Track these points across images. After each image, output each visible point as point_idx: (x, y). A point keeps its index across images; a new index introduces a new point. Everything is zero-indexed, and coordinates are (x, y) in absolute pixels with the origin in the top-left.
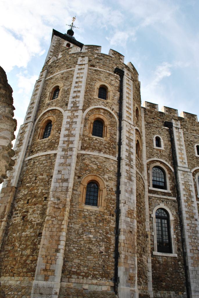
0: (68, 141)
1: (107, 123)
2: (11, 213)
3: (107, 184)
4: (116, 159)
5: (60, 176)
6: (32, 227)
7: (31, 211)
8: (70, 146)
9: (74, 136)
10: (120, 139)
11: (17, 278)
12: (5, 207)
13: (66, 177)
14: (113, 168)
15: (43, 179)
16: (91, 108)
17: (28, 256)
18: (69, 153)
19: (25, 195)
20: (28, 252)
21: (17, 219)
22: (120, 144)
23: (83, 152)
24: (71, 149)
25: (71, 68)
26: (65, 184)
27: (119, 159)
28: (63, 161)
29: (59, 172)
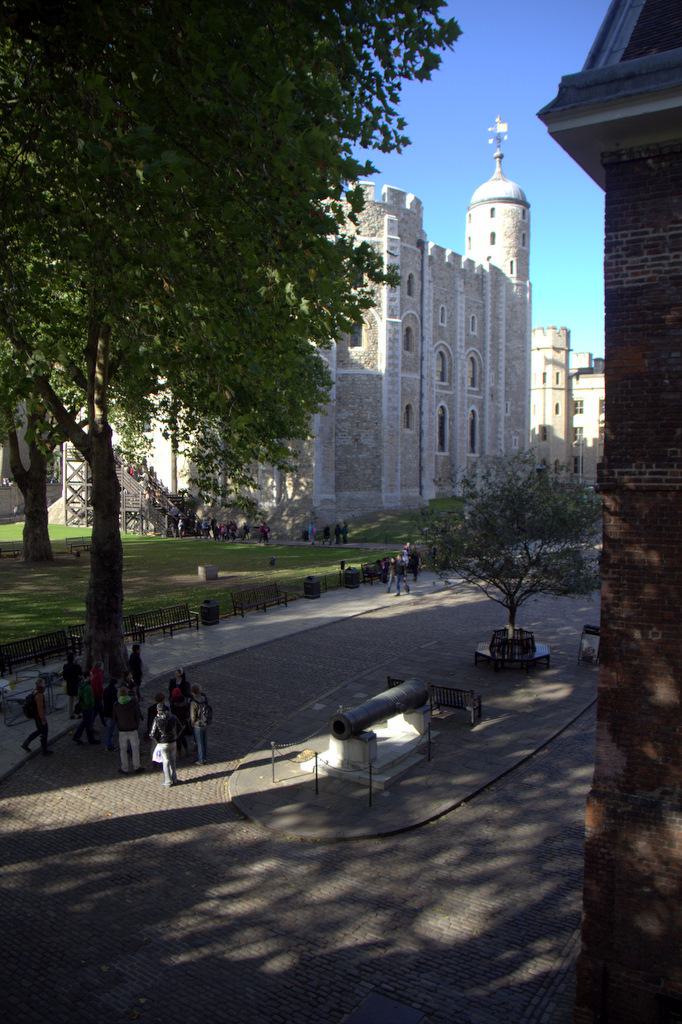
0: (393, 364)
1: (414, 333)
2: (336, 434)
3: (415, 408)
4: (419, 378)
5: (391, 404)
6: (368, 450)
7: (363, 435)
8: (396, 370)
9: (398, 358)
10: (422, 353)
11: (363, 492)
12: (331, 429)
13: (396, 405)
14: (418, 390)
15: (370, 403)
16: (405, 314)
17: (370, 475)
18: (396, 379)
19: (349, 417)
20: (370, 471)
21: (349, 441)
22: (422, 359)
23: (405, 375)
24: (397, 374)
25: (373, 235)
26: (395, 413)
27: (422, 377)
28: (391, 387)
29: (390, 399)
